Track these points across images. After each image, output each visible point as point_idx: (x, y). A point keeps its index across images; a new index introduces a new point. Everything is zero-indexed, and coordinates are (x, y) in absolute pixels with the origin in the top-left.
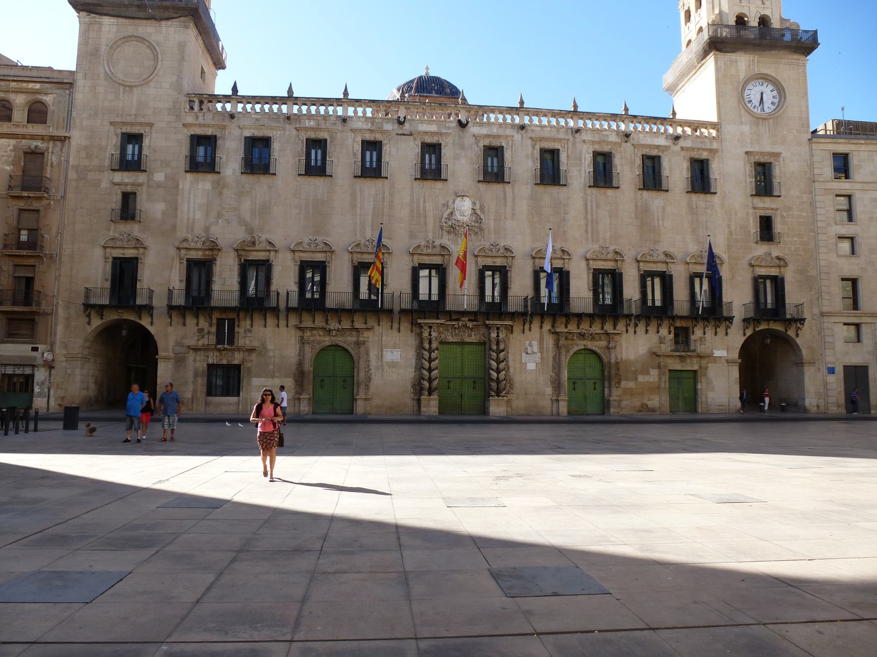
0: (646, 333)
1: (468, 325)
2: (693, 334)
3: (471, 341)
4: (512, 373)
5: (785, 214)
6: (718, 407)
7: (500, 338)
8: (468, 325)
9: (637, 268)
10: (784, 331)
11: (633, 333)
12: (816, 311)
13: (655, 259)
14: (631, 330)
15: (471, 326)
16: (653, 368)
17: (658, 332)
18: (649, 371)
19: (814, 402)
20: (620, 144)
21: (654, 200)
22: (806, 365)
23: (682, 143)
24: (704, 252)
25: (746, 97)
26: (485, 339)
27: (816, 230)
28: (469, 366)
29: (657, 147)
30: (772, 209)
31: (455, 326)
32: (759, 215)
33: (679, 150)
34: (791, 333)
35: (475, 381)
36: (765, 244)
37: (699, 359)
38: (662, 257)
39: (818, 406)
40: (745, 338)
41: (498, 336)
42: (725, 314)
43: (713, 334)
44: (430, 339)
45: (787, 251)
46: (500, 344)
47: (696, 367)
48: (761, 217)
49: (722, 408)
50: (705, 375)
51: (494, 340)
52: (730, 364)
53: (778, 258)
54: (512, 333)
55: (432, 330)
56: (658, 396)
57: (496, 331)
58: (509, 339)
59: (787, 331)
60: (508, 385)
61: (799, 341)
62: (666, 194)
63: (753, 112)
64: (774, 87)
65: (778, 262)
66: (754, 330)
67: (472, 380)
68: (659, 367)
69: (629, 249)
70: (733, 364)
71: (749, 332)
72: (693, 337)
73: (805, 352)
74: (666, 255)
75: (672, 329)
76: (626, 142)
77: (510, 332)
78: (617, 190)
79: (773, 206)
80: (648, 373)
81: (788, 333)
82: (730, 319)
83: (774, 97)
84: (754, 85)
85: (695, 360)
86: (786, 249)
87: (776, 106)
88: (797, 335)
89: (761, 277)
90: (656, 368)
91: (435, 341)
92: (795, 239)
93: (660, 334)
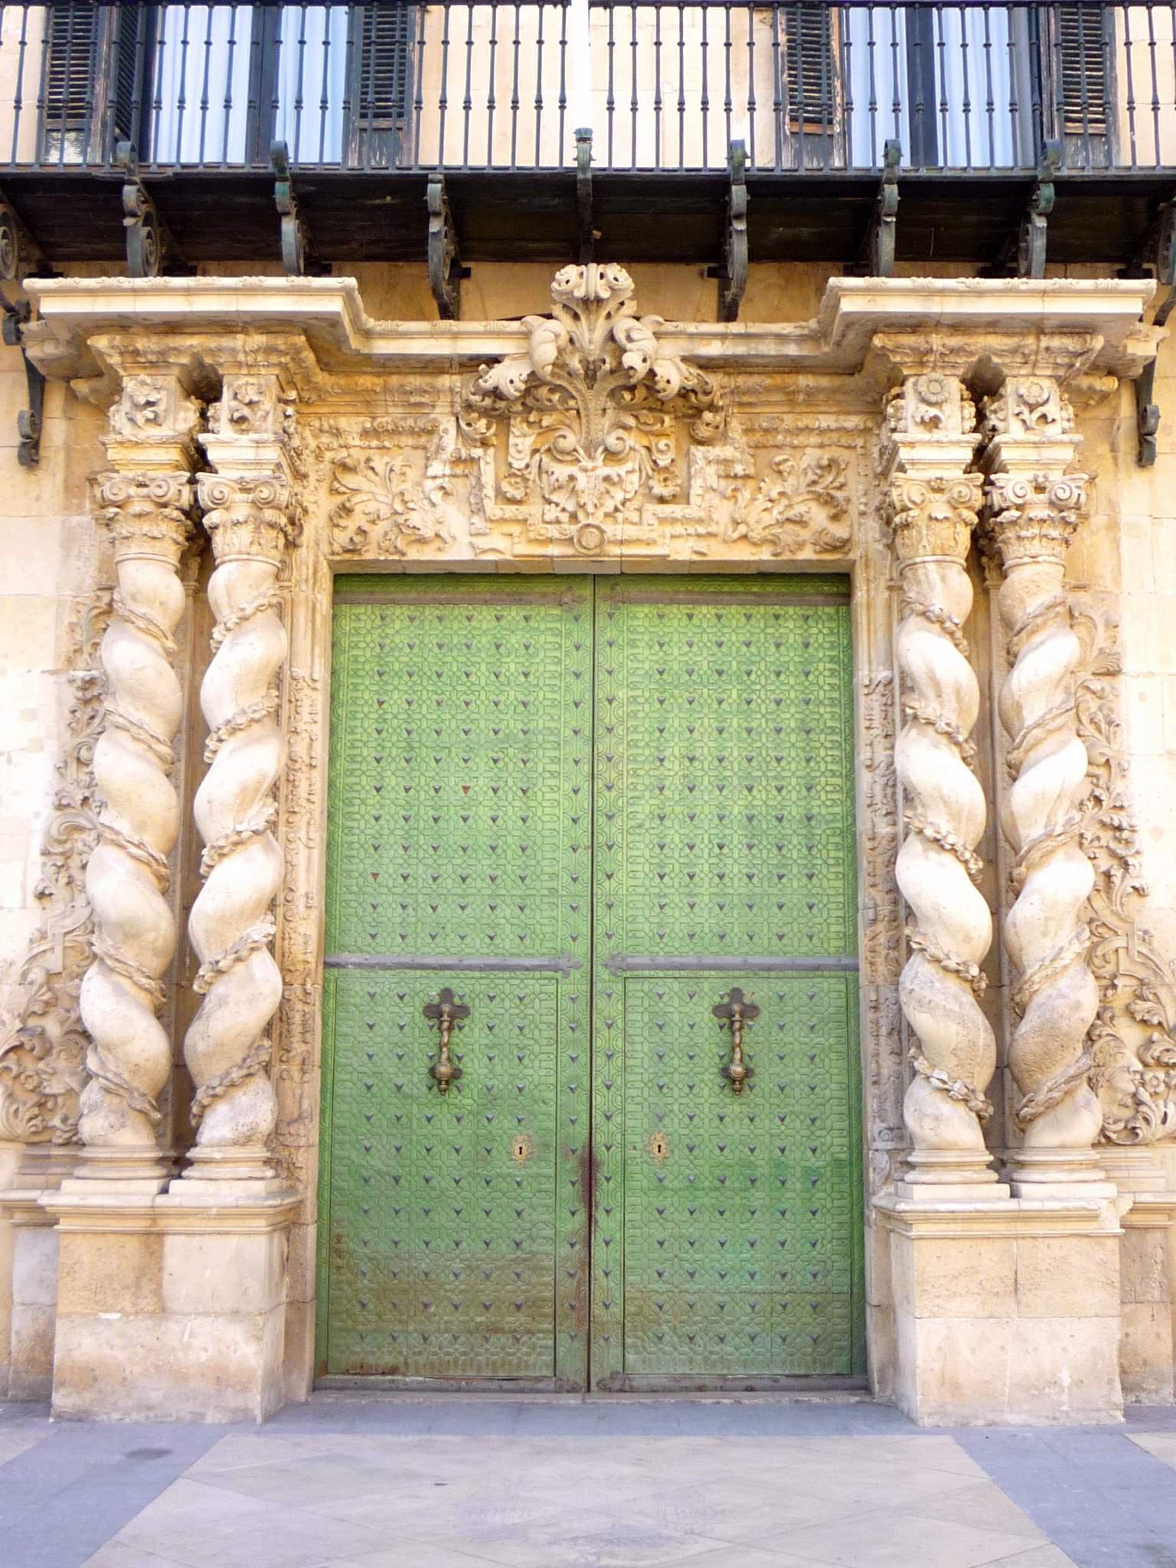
1: (631, 359)
3: (682, 551)
4: (1157, 898)
7: (1012, 484)
8: (631, 359)
15: (673, 375)
26: (840, 531)
28: (674, 836)
31: (495, 377)
35: (736, 994)
41: (984, 460)
44: (195, 513)
46: (1013, 552)
51: (940, 508)
54: (1145, 455)
55: (223, 408)
57: (957, 415)
58: (1113, 526)
60: (1131, 1035)
67: (713, 990)
77: (1127, 445)
91: (245, 534)
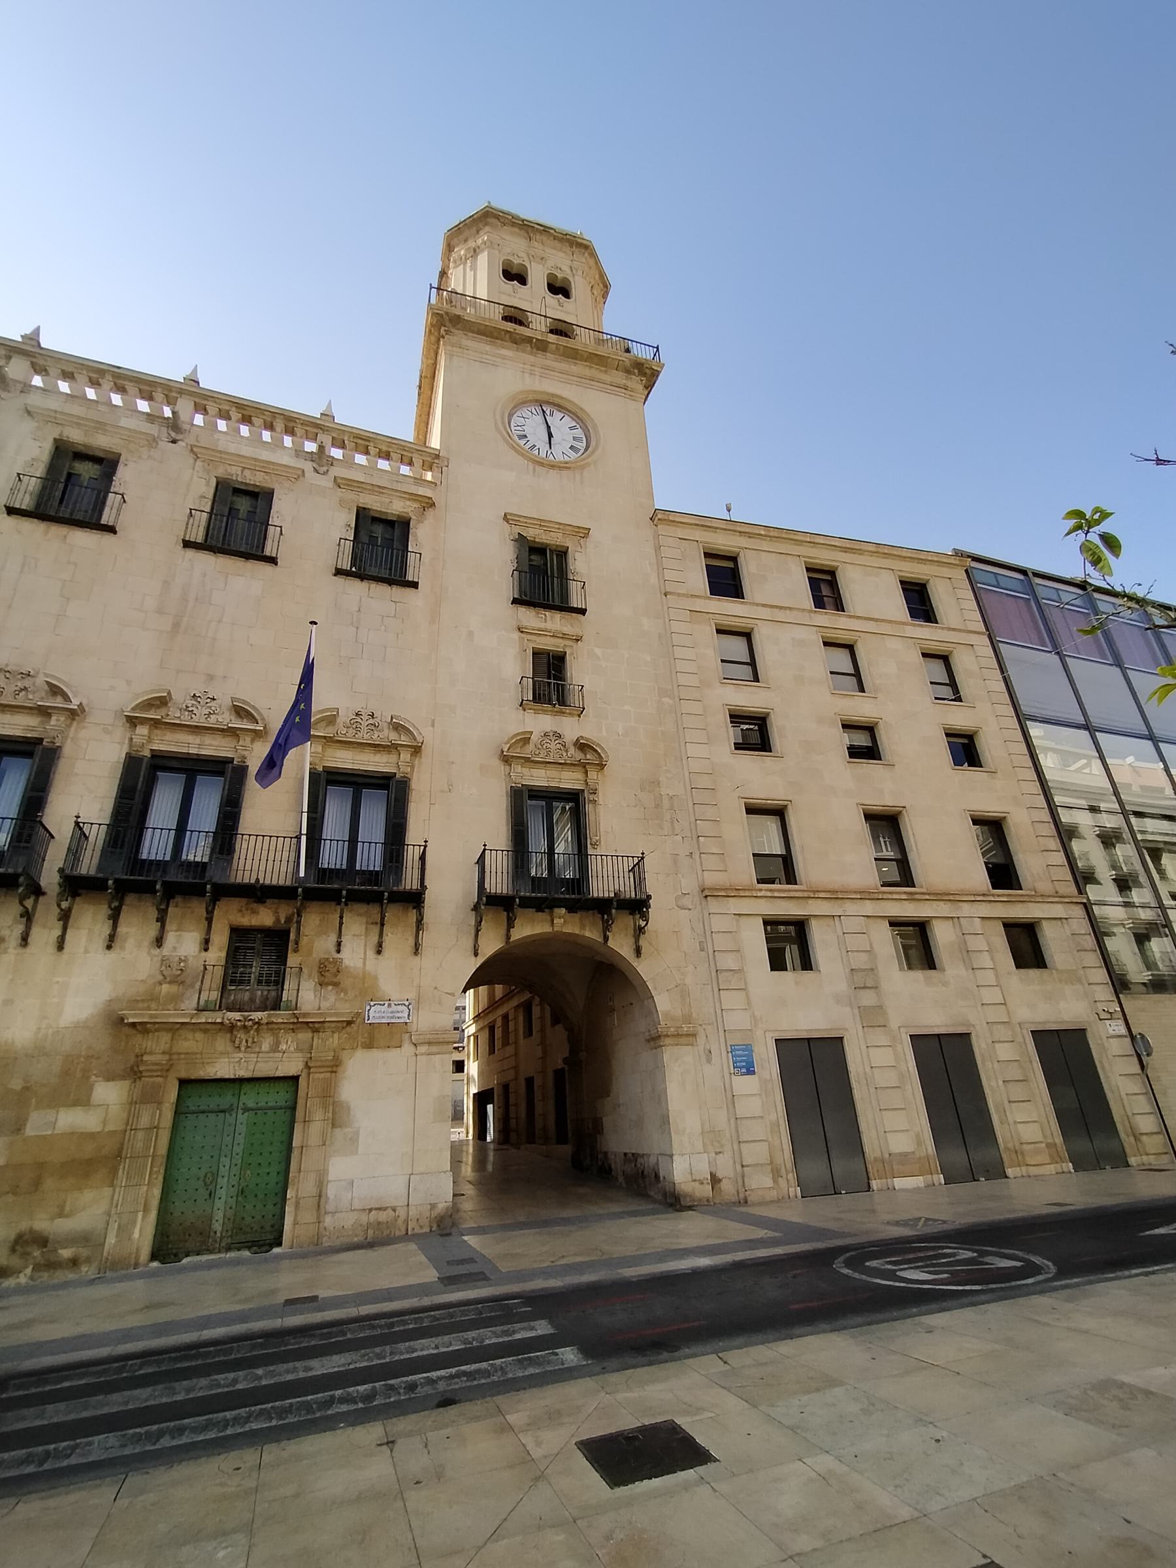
0: (109, 947)
2: (296, 951)
5: (598, 651)
6: (364, 1219)
9: (127, 741)
10: (601, 940)
11: (51, 949)
12: (689, 884)
13: (199, 719)
14: (44, 934)
16: (110, 1077)
17: (159, 942)
18: (91, 1088)
19: (703, 1169)
20: (153, 441)
21: (230, 576)
22: (667, 1041)
23: (336, 471)
24: (365, 717)
25: (512, 427)
27: (676, 694)
29: (267, 467)
30: (564, 636)
32: (532, 645)
33: (331, 484)
34: (620, 944)
36: (545, 712)
37: (304, 1036)
38: (227, 719)
39: (715, 1180)
40: (480, 961)
42: (410, 881)
43: (371, 953)
45: (604, 732)
47: (290, 1066)
48: (536, 654)
49: (383, 1217)
50: (328, 1096)
52: (423, 1049)
53: (583, 746)
56: (107, 1191)
59: (606, 939)
61: (644, 968)
62: (267, 568)
63: (518, 445)
64: (578, 423)
65: (579, 756)
66: (508, 937)
68: (134, 1073)
69: (112, 688)
70: (434, 1049)
71: (491, 944)
72: (293, 960)
73: (664, 1003)
74: (240, 711)
75: (220, 939)
76: (174, 442)
78: (107, 538)
79: (567, 629)
80: (83, 1100)
81: (610, 943)
82: (415, 899)
83: (574, 438)
84: (534, 411)
85: (288, 1042)
86: (604, 728)
87: (579, 455)
88: (638, 952)
89: (535, 793)
90: (123, 1078)
92: (626, 708)
93: (166, 950)
